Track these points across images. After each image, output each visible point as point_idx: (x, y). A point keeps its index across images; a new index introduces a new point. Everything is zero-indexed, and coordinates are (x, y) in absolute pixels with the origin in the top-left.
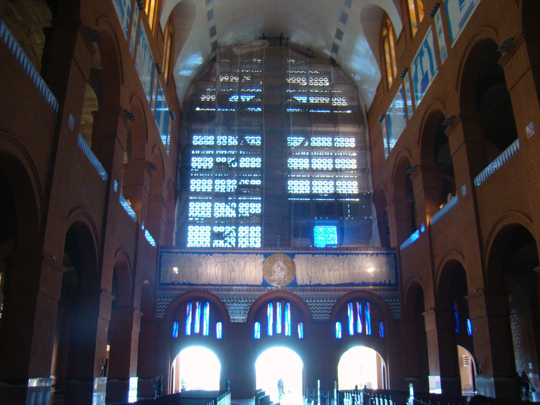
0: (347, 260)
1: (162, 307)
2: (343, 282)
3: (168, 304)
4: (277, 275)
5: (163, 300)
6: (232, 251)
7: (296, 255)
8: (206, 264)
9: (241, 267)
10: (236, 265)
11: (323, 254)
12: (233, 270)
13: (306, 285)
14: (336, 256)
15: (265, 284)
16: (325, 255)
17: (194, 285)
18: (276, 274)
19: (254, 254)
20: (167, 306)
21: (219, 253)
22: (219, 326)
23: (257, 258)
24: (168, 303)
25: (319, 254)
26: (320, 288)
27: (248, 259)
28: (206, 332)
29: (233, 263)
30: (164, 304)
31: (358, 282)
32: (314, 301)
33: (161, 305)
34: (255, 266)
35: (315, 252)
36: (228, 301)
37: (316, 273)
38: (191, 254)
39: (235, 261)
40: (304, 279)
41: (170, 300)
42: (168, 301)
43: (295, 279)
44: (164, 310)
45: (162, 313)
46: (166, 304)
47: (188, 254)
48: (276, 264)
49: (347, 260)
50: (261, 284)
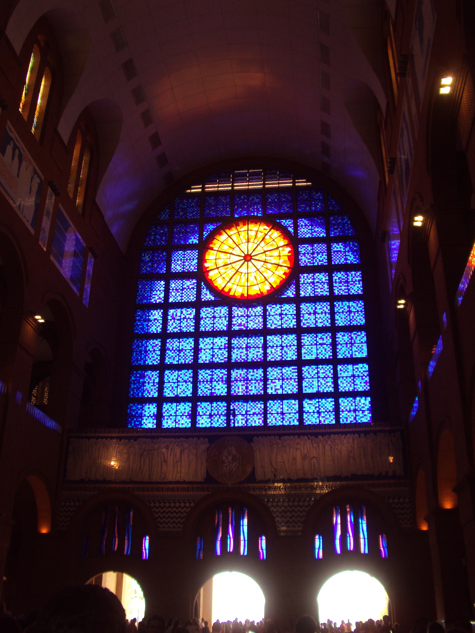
0: (329, 443)
4: (227, 468)
6: (165, 434)
7: (255, 438)
9: (176, 456)
10: (169, 454)
11: (294, 435)
12: (165, 461)
14: (314, 437)
15: (209, 479)
16: (296, 436)
17: (110, 482)
18: (225, 465)
19: (195, 438)
21: (147, 437)
25: (289, 435)
27: (186, 445)
34: (196, 455)
35: (283, 432)
37: (284, 462)
38: (109, 439)
39: (168, 449)
43: (253, 472)
47: (104, 440)
48: (226, 451)
49: (329, 443)
50: (203, 481)
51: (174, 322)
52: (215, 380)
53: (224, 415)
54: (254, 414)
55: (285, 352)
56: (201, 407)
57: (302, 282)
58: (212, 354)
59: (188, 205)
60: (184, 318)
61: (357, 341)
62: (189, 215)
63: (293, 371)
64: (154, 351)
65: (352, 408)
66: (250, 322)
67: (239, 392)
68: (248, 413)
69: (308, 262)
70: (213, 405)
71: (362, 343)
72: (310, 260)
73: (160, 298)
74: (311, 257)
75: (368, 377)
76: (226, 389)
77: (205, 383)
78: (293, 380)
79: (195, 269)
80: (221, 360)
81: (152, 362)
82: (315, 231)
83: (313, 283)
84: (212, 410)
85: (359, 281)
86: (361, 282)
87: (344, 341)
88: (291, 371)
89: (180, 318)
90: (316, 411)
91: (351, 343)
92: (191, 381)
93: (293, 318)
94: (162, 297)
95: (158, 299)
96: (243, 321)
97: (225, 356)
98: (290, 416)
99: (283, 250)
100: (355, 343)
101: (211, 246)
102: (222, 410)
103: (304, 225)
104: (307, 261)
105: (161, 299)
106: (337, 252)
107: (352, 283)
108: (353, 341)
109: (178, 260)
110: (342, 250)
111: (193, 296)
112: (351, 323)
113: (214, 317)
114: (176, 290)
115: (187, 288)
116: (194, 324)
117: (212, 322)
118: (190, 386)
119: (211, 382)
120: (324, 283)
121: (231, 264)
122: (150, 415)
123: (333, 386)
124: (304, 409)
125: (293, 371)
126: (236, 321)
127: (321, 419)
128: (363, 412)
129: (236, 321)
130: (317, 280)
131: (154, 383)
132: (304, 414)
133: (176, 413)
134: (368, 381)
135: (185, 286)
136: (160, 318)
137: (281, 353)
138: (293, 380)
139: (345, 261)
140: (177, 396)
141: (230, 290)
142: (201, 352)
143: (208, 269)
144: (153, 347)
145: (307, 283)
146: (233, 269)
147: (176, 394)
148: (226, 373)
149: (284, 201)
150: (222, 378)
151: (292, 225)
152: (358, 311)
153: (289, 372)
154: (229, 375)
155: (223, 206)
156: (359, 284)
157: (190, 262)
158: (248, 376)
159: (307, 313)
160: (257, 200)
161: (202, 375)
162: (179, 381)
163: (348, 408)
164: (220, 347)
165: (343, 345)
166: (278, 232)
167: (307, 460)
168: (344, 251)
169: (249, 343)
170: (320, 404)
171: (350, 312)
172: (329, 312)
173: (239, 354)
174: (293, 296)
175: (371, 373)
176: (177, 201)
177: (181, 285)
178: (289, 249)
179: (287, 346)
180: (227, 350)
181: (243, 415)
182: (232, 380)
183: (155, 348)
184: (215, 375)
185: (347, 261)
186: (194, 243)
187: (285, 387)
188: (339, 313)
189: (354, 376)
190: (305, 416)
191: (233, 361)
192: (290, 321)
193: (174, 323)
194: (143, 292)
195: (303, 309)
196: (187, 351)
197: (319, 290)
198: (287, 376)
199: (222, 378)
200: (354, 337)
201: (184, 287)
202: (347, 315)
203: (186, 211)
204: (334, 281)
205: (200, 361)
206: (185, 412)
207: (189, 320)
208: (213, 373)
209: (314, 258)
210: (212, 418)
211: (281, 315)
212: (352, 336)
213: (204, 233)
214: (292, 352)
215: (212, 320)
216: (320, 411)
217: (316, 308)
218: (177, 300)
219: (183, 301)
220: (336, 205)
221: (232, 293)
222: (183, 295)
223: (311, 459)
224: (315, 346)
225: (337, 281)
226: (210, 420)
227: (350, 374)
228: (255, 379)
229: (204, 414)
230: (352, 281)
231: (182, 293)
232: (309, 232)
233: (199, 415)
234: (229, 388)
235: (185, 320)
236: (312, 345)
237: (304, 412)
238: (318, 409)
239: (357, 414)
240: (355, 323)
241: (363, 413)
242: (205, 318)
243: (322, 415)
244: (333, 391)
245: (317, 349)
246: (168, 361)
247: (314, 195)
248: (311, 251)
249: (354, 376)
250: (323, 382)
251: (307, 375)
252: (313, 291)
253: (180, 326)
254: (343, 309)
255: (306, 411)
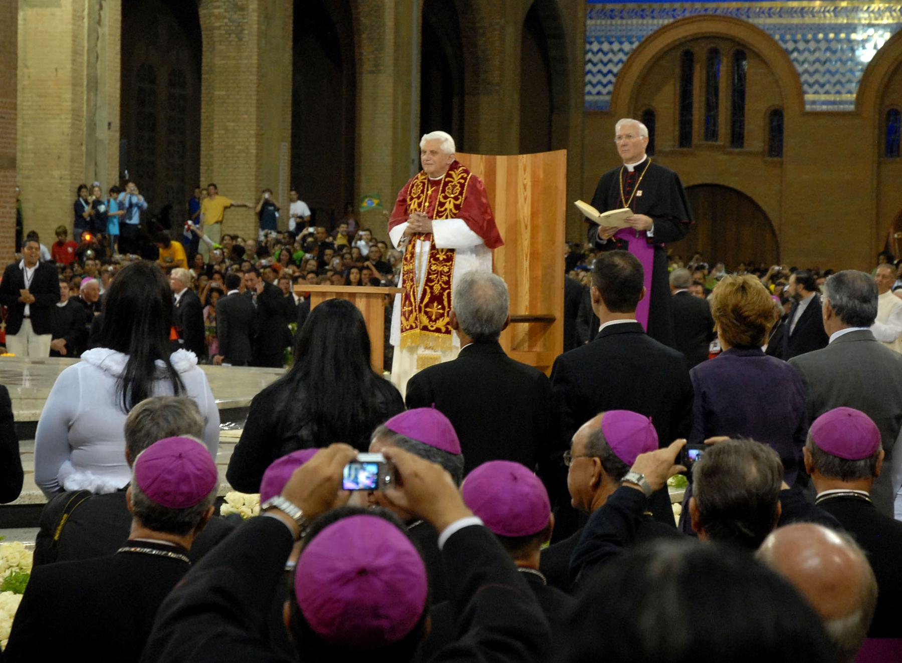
1: (605, 70)
3: (620, 61)
5: (606, 47)
20: (620, 66)
24: (621, 56)
30: (610, 61)
33: (601, 61)
36: (801, 46)
41: (627, 47)
42: (621, 50)
44: (610, 77)
45: (605, 86)
46: (616, 59)
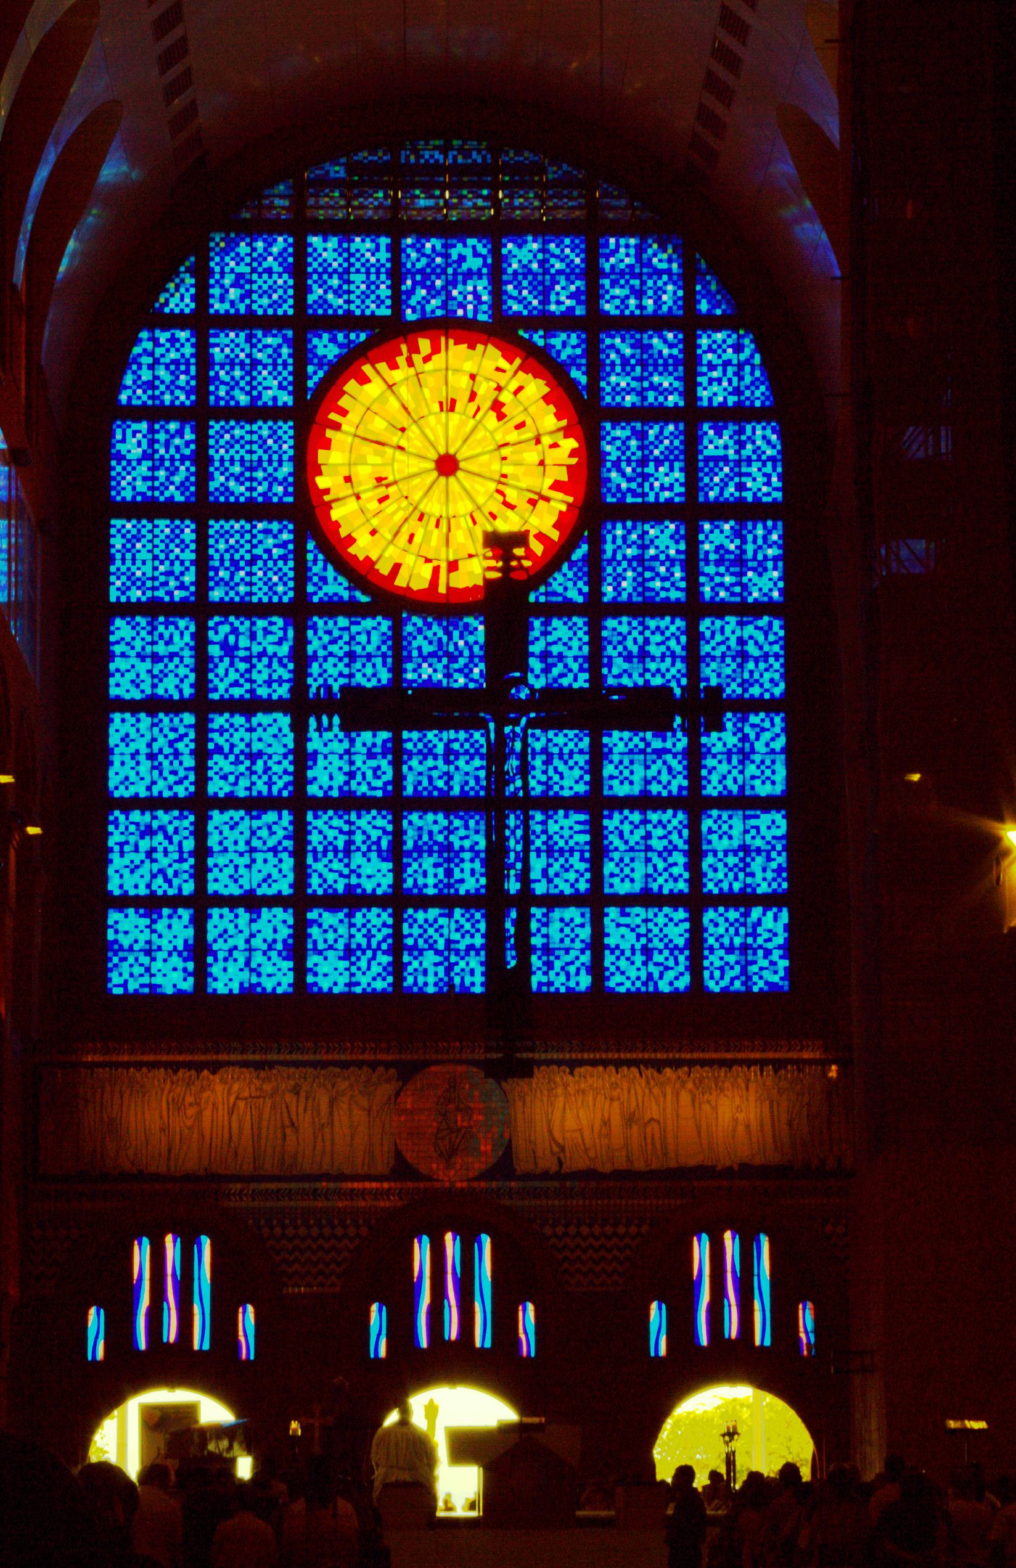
2: (672, 1164)
8: (199, 1104)
9: (319, 1114)
12: (293, 1124)
13: (545, 1175)
15: (401, 1169)
19: (365, 1068)
22: (248, 1319)
23: (374, 1079)
26: (593, 1184)
27: (343, 1085)
28: (201, 1340)
29: (290, 1098)
31: (728, 1164)
32: (572, 1230)
38: (144, 1070)
39: (298, 1094)
40: (539, 1154)
49: (690, 1085)
51: (232, 664)
52: (358, 849)
53: (384, 953)
54: (470, 947)
55: (556, 769)
56: (320, 926)
57: (609, 554)
58: (346, 769)
59: (255, 264)
60: (263, 654)
61: (759, 746)
62: (260, 302)
63: (577, 828)
64: (177, 754)
65: (737, 941)
66: (456, 675)
67: (426, 886)
68: (453, 946)
69: (629, 490)
70: (353, 921)
71: (773, 751)
72: (633, 485)
73: (182, 587)
74: (639, 475)
75: (784, 854)
76: (390, 875)
77: (330, 855)
78: (577, 855)
79: (286, 493)
80: (375, 789)
81: (170, 788)
82: (651, 383)
83: (640, 559)
84: (352, 936)
85: (775, 559)
86: (780, 564)
87: (725, 745)
88: (571, 828)
89: (247, 653)
90: (638, 946)
91: (741, 751)
92: (291, 848)
93: (581, 670)
94: (192, 584)
95: (177, 588)
96: (435, 671)
97: (385, 778)
98: (568, 958)
99: (555, 445)
100: (753, 751)
101: (333, 416)
102: (380, 937)
103: (618, 362)
104: (624, 486)
105: (187, 589)
106: (716, 459)
107: (755, 564)
108: (747, 745)
109: (232, 461)
110: (731, 453)
111: (285, 584)
112: (745, 690)
113: (352, 656)
114: (234, 563)
115: (265, 556)
116: (291, 676)
117: (346, 671)
118: (288, 863)
119: (347, 852)
120: (673, 562)
121: (395, 482)
122: (175, 948)
123: (686, 875)
124: (607, 941)
125: (577, 828)
126: (414, 670)
127: (651, 968)
128: (768, 953)
129: (414, 670)
130: (652, 552)
131: (181, 851)
132: (607, 952)
133: (247, 941)
134: (784, 865)
135: (258, 551)
136: (187, 653)
137: (545, 772)
138: (577, 855)
139: (737, 494)
140: (252, 892)
141: (397, 567)
142: (315, 763)
143: (326, 498)
144: (171, 743)
145: (624, 557)
146: (405, 503)
147: (247, 887)
148: (390, 828)
149: (560, 272)
150: (378, 842)
151: (584, 361)
152: (766, 656)
153: (566, 833)
154: (398, 834)
155: (368, 278)
156: (775, 568)
157: (270, 470)
158: (452, 838)
159: (620, 655)
160: (474, 263)
161: (320, 832)
162: (253, 850)
163: (726, 941)
164: (369, 750)
165: (719, 757)
166: (541, 382)
167: (635, 1128)
168: (737, 457)
169: (457, 740)
170: (650, 925)
171: (745, 656)
172: (684, 653)
173: (426, 773)
174: (580, 599)
175: (792, 841)
176: (217, 244)
177: (248, 546)
178: (572, 444)
179: (561, 755)
180: (390, 757)
181: (438, 953)
182: (405, 848)
183: (180, 746)
184: (359, 832)
185: (744, 494)
186: (280, 403)
187: (557, 875)
188: (714, 659)
189: (745, 848)
190: (609, 959)
191: (410, 790)
192: (571, 676)
193: (232, 670)
194: (129, 563)
195: (610, 643)
196: (276, 758)
197: (657, 584)
198: (561, 843)
199: (378, 842)
200: (752, 736)
201: (255, 551)
202: (734, 666)
203: (247, 287)
204: (702, 556)
205: (313, 790)
206: (275, 941)
207: (275, 660)
208: (353, 828)
209: (646, 477)
210: (353, 959)
211: (544, 656)
212: (747, 729)
213: (310, 369)
214: (577, 773)
215: (346, 665)
216: (650, 946)
217: (647, 641)
218: (237, 593)
219: (255, 599)
220: (719, 297)
221: (400, 582)
222: (255, 579)
223: (646, 1124)
224: (642, 757)
225: (713, 557)
226: (346, 964)
227: (736, 843)
228: (472, 849)
229: (331, 947)
230: (755, 558)
231: (250, 574)
232: (633, 389)
233: (315, 948)
234: (399, 871)
235: (265, 660)
236: (631, 752)
237: (608, 947)
238: (643, 940)
239: (750, 958)
240: (756, 691)
241: (765, 957)
242: (325, 659)
243: (658, 958)
244: (686, 890)
245: (647, 767)
246: (217, 787)
247: (655, 255)
248: (639, 453)
249: (745, 848)
250: (661, 865)
251: (617, 842)
252: (640, 584)
253: (251, 681)
254: (723, 648)
255: (613, 946)
